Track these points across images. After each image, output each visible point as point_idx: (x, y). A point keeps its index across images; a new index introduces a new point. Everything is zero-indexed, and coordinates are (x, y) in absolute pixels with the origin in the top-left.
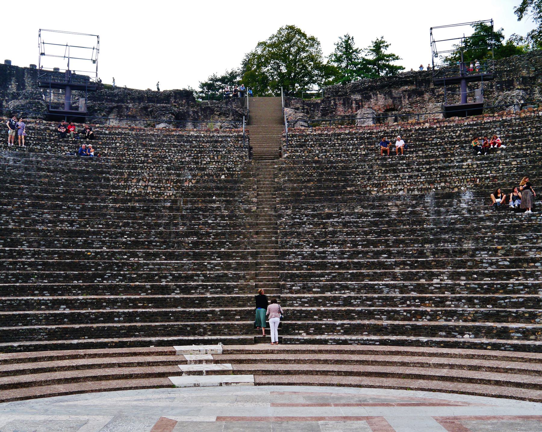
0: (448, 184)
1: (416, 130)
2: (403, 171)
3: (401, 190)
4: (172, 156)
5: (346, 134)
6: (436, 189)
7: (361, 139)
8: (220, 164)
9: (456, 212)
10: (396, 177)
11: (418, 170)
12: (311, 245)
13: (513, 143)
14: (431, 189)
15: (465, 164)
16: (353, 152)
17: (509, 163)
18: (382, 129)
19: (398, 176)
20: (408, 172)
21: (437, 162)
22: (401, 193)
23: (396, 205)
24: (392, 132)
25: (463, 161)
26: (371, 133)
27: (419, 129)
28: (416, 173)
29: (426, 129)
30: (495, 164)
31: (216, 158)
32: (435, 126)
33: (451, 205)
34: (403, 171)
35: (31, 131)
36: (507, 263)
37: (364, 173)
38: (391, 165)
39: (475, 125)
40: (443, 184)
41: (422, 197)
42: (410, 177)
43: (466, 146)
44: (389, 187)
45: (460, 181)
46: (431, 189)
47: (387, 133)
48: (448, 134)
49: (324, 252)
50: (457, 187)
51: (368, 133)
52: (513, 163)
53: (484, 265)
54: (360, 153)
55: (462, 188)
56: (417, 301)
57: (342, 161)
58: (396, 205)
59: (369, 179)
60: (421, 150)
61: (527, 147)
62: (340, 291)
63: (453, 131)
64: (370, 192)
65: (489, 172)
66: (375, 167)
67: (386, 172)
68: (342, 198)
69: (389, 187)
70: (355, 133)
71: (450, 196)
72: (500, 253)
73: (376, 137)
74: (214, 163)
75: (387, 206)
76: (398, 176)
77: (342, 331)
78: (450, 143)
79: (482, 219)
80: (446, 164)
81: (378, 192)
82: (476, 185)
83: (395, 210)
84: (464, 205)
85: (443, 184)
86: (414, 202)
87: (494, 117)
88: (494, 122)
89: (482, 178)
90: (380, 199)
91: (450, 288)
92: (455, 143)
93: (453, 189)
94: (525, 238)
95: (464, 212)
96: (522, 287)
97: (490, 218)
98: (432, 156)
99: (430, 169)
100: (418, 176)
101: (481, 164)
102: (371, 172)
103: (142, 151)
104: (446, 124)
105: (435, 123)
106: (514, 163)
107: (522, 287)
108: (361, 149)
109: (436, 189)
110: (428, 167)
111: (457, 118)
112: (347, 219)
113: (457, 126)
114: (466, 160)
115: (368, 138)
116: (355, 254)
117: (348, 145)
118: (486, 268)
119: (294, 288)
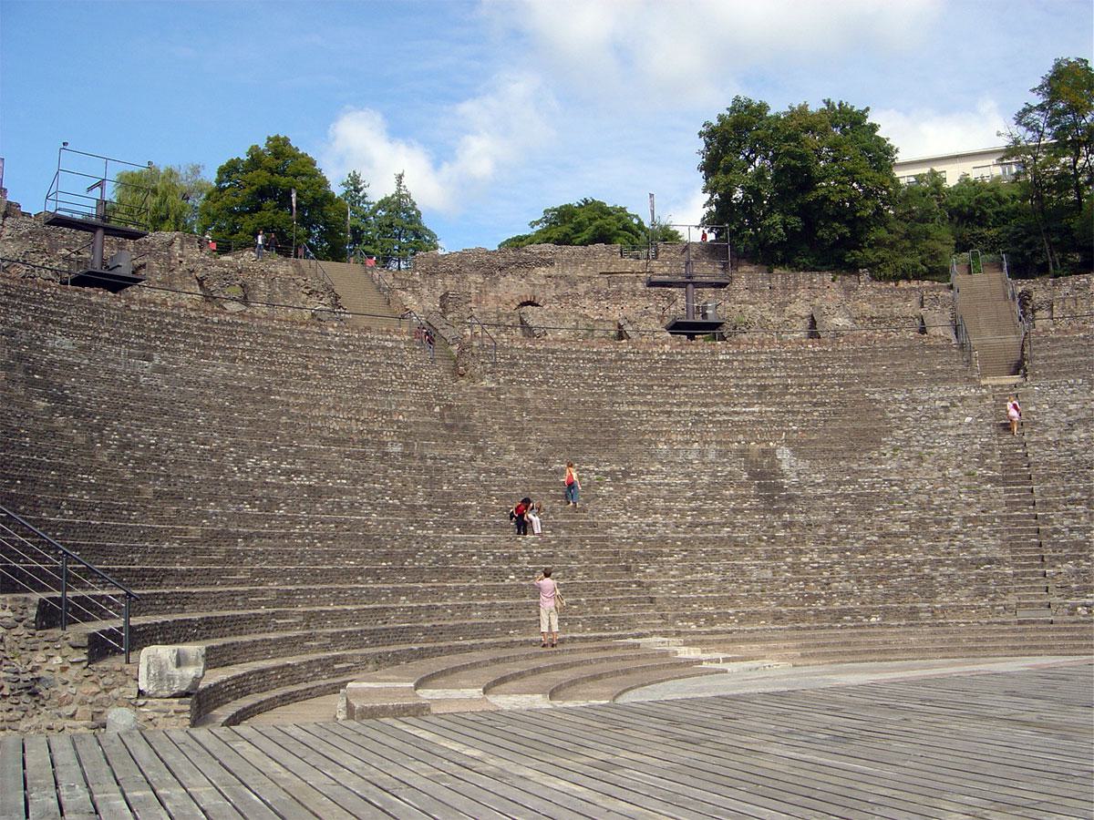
4: (342, 370)
8: (417, 387)
17: (811, 412)
31: (404, 377)
35: (112, 312)
36: (875, 538)
43: (742, 385)
52: (815, 414)
53: (850, 540)
54: (604, 383)
56: (801, 583)
62: (702, 573)
65: (791, 424)
74: (410, 386)
77: (736, 621)
89: (789, 431)
91: (829, 567)
94: (881, 509)
96: (906, 565)
103: (290, 358)
106: (815, 414)
107: (906, 565)
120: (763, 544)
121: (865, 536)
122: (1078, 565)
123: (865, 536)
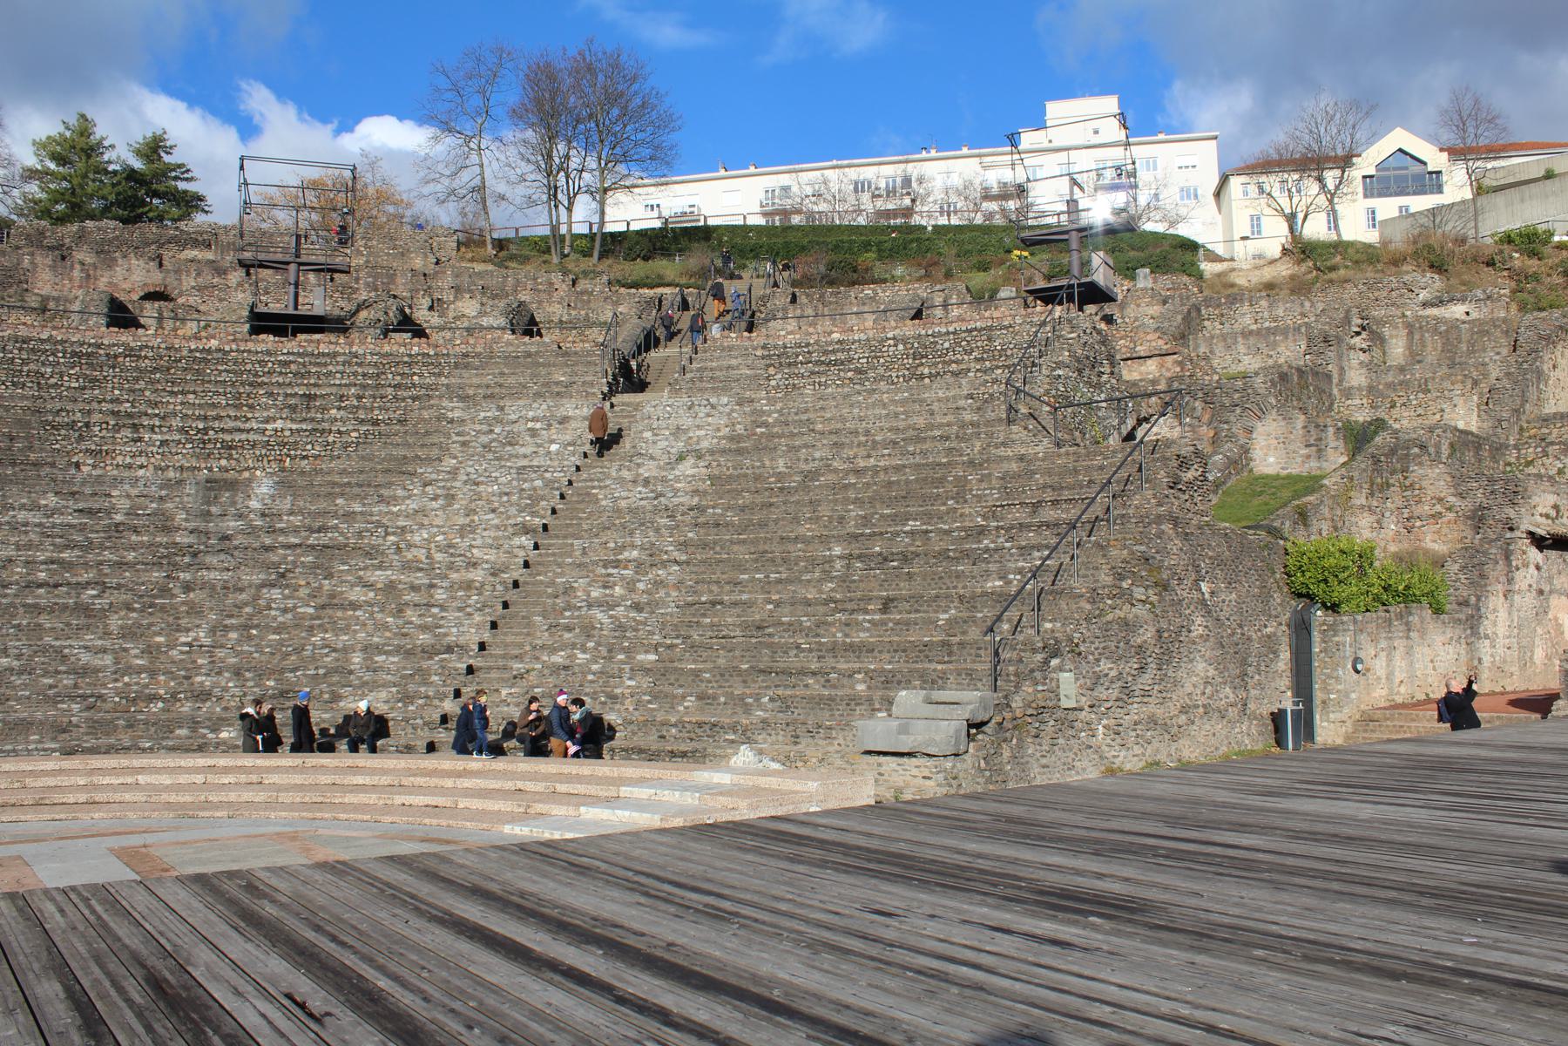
0: (234, 463)
1: (191, 351)
2: (152, 429)
3: (141, 467)
5: (43, 341)
6: (210, 470)
7: (74, 354)
9: (241, 516)
10: (135, 441)
11: (182, 430)
13: (359, 398)
14: (199, 469)
15: (269, 427)
16: (53, 381)
17: (348, 433)
18: (124, 338)
19: (140, 440)
20: (161, 433)
21: (219, 418)
22: (141, 472)
23: (128, 496)
24: (141, 348)
25: (267, 421)
26: (99, 346)
27: (197, 350)
28: (177, 437)
29: (209, 351)
30: (323, 431)
32: (227, 348)
33: (234, 503)
34: (152, 429)
36: (311, 610)
37: (72, 425)
38: (129, 415)
39: (299, 354)
40: (224, 462)
41: (180, 482)
42: (164, 443)
44: (119, 459)
45: (259, 458)
46: (199, 469)
47: (132, 349)
48: (249, 367)
50: (247, 469)
51: (90, 345)
53: (273, 613)
55: (258, 473)
57: (23, 397)
58: (128, 496)
59: (81, 438)
60: (194, 392)
61: (380, 408)
63: (259, 362)
64: (77, 465)
66: (96, 417)
67: (117, 428)
68: (14, 474)
69: (119, 459)
70: (63, 342)
71: (232, 485)
72: (303, 592)
73: (107, 355)
75: (109, 495)
76: (140, 440)
78: (251, 384)
79: (282, 531)
80: (239, 424)
81: (94, 467)
82: (283, 470)
83: (124, 504)
84: (254, 504)
85: (224, 462)
86: (163, 493)
87: (337, 344)
88: (335, 354)
90: (99, 480)
92: (261, 385)
93: (240, 472)
95: (252, 516)
97: (296, 531)
98: (214, 406)
99: (205, 431)
100: (179, 442)
101: (298, 431)
102: (87, 425)
104: (250, 346)
105: (229, 342)
108: (70, 376)
109: (210, 470)
110: (201, 426)
111: (271, 337)
112: (22, 516)
113: (269, 353)
114: (275, 420)
115: (89, 355)
116: (31, 585)
117: (43, 364)
118: (275, 618)
120: (134, 615)
121: (295, 607)
122: (572, 657)
123: (295, 607)
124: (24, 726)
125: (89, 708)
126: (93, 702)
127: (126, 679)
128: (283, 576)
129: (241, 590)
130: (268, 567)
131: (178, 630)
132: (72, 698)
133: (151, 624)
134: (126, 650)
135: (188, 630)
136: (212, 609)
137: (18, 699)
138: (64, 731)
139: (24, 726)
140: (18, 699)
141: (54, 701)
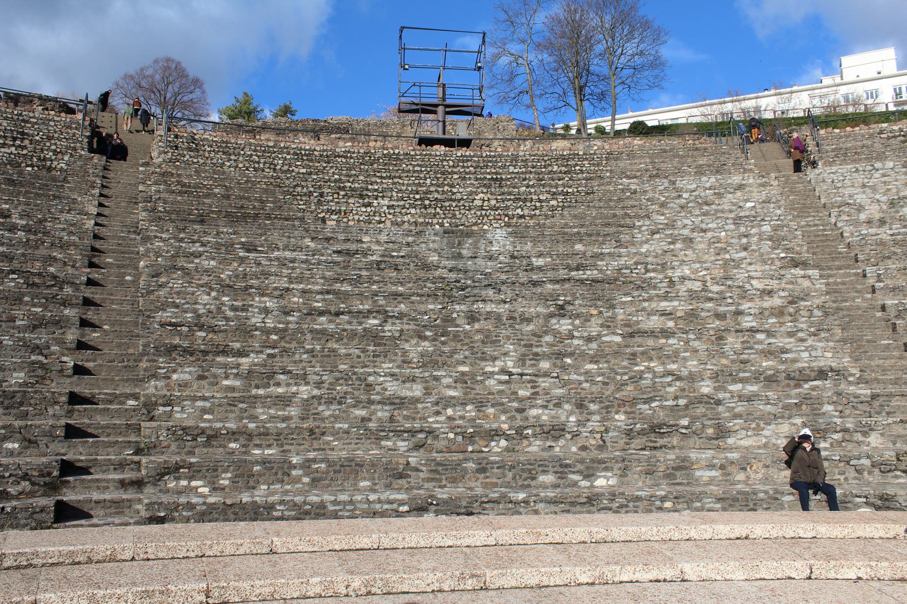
12: (214, 294)
49: (244, 309)
119: (175, 376)
124: (350, 468)
125: (418, 447)
126: (423, 439)
127: (450, 412)
128: (562, 307)
129: (529, 320)
130: (544, 299)
131: (483, 359)
132: (398, 433)
133: (454, 352)
134: (437, 379)
135: (494, 359)
136: (508, 338)
137: (336, 433)
138: (401, 476)
139: (350, 468)
140: (336, 433)
141: (376, 437)
